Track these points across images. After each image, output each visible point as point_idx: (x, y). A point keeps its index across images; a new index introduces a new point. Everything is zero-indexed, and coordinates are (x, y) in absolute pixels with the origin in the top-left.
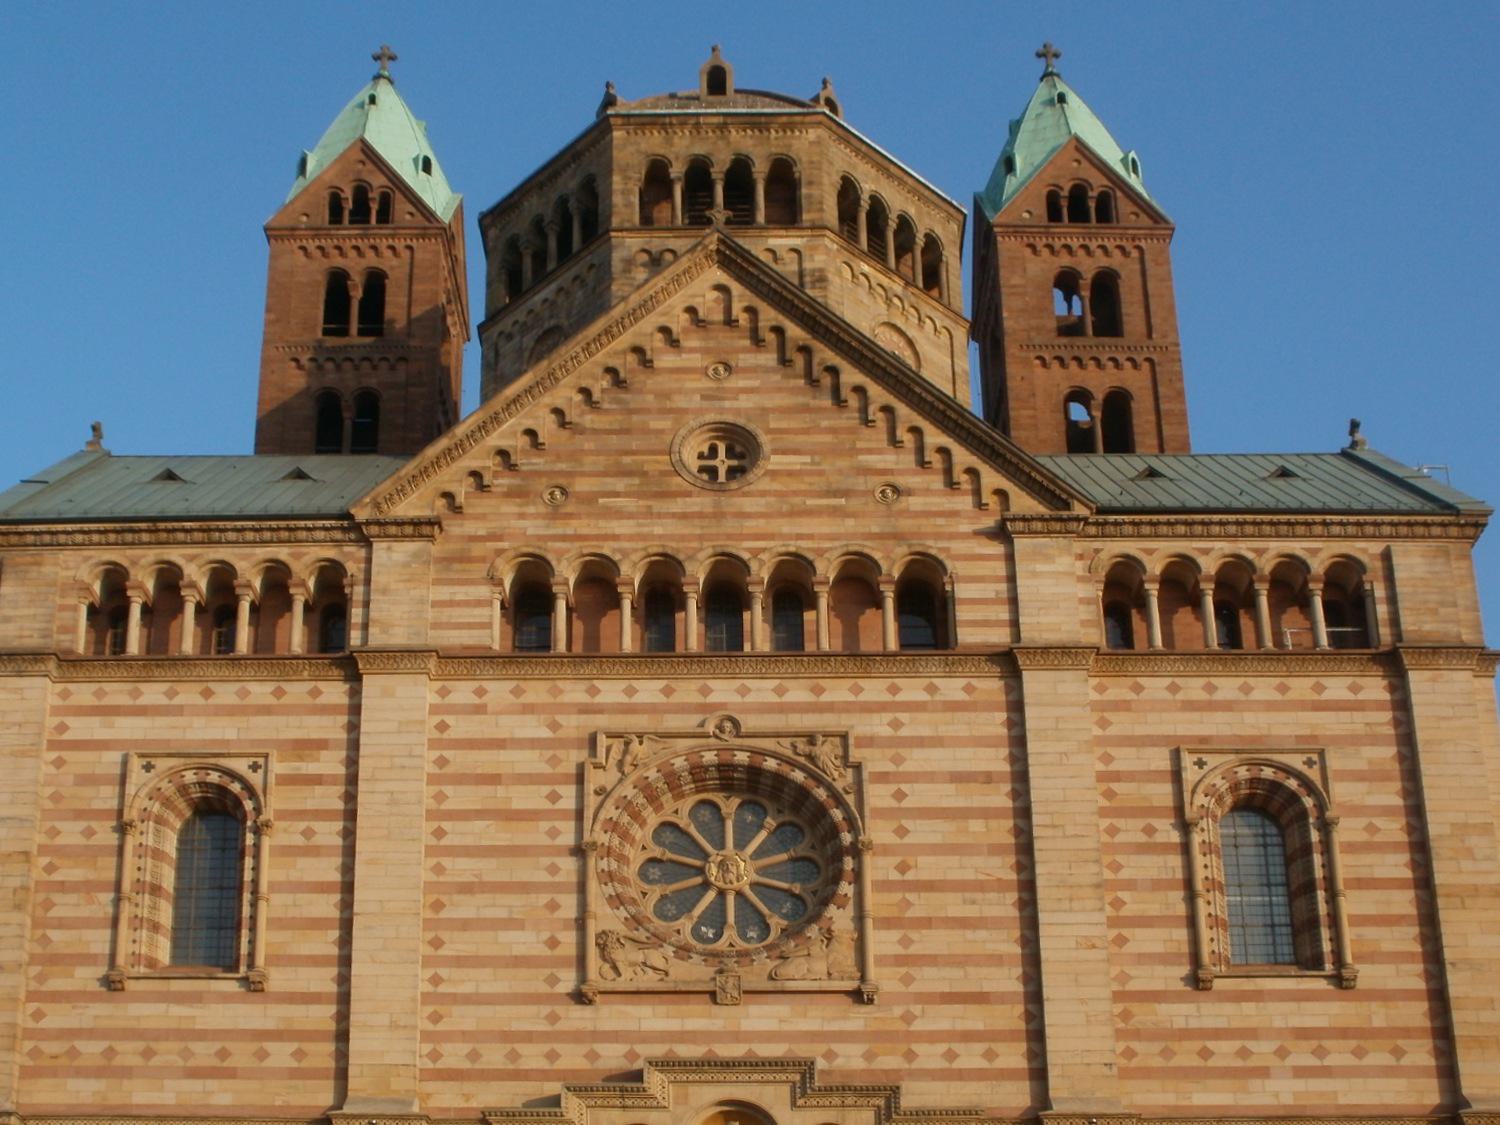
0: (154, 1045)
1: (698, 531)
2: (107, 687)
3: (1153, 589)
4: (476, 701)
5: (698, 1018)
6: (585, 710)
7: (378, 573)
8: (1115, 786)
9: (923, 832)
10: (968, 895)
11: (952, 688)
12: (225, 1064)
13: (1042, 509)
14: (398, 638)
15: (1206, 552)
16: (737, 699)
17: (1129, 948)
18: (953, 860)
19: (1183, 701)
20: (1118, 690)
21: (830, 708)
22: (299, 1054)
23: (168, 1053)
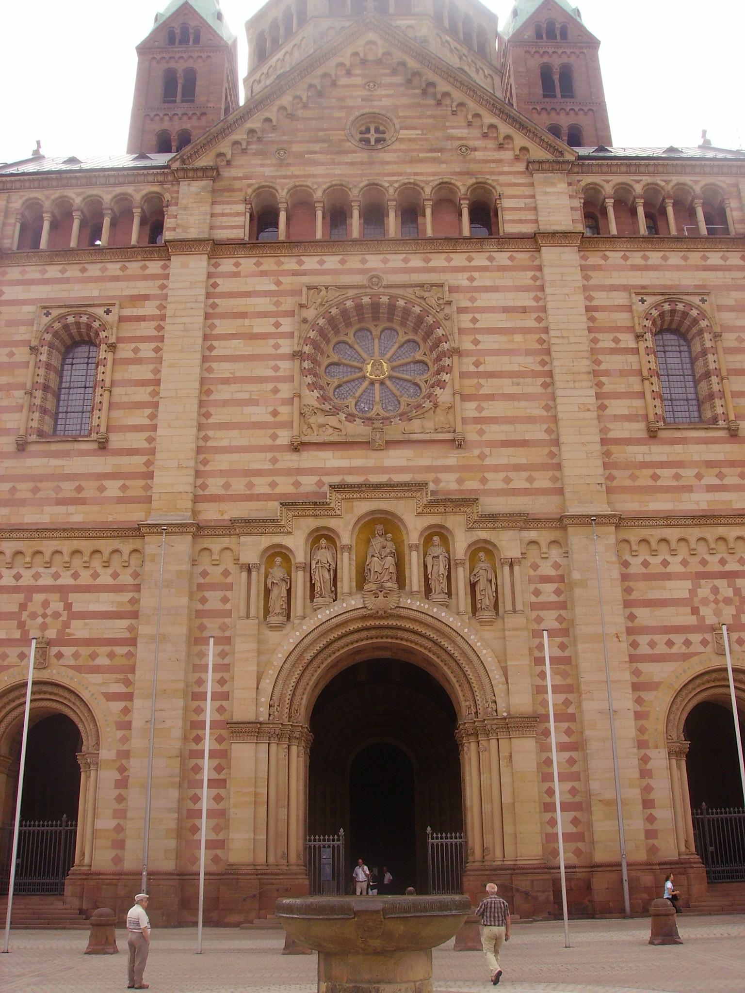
0: (39, 485)
1: (360, 172)
2: (27, 268)
3: (610, 202)
4: (235, 269)
5: (359, 459)
6: (295, 273)
7: (183, 198)
8: (595, 314)
9: (489, 342)
10: (515, 380)
11: (502, 258)
12: (80, 496)
13: (548, 156)
14: (193, 234)
15: (638, 182)
16: (382, 265)
17: (609, 412)
18: (506, 359)
19: (632, 265)
20: (594, 259)
21: (434, 270)
22: (124, 488)
23: (47, 489)
